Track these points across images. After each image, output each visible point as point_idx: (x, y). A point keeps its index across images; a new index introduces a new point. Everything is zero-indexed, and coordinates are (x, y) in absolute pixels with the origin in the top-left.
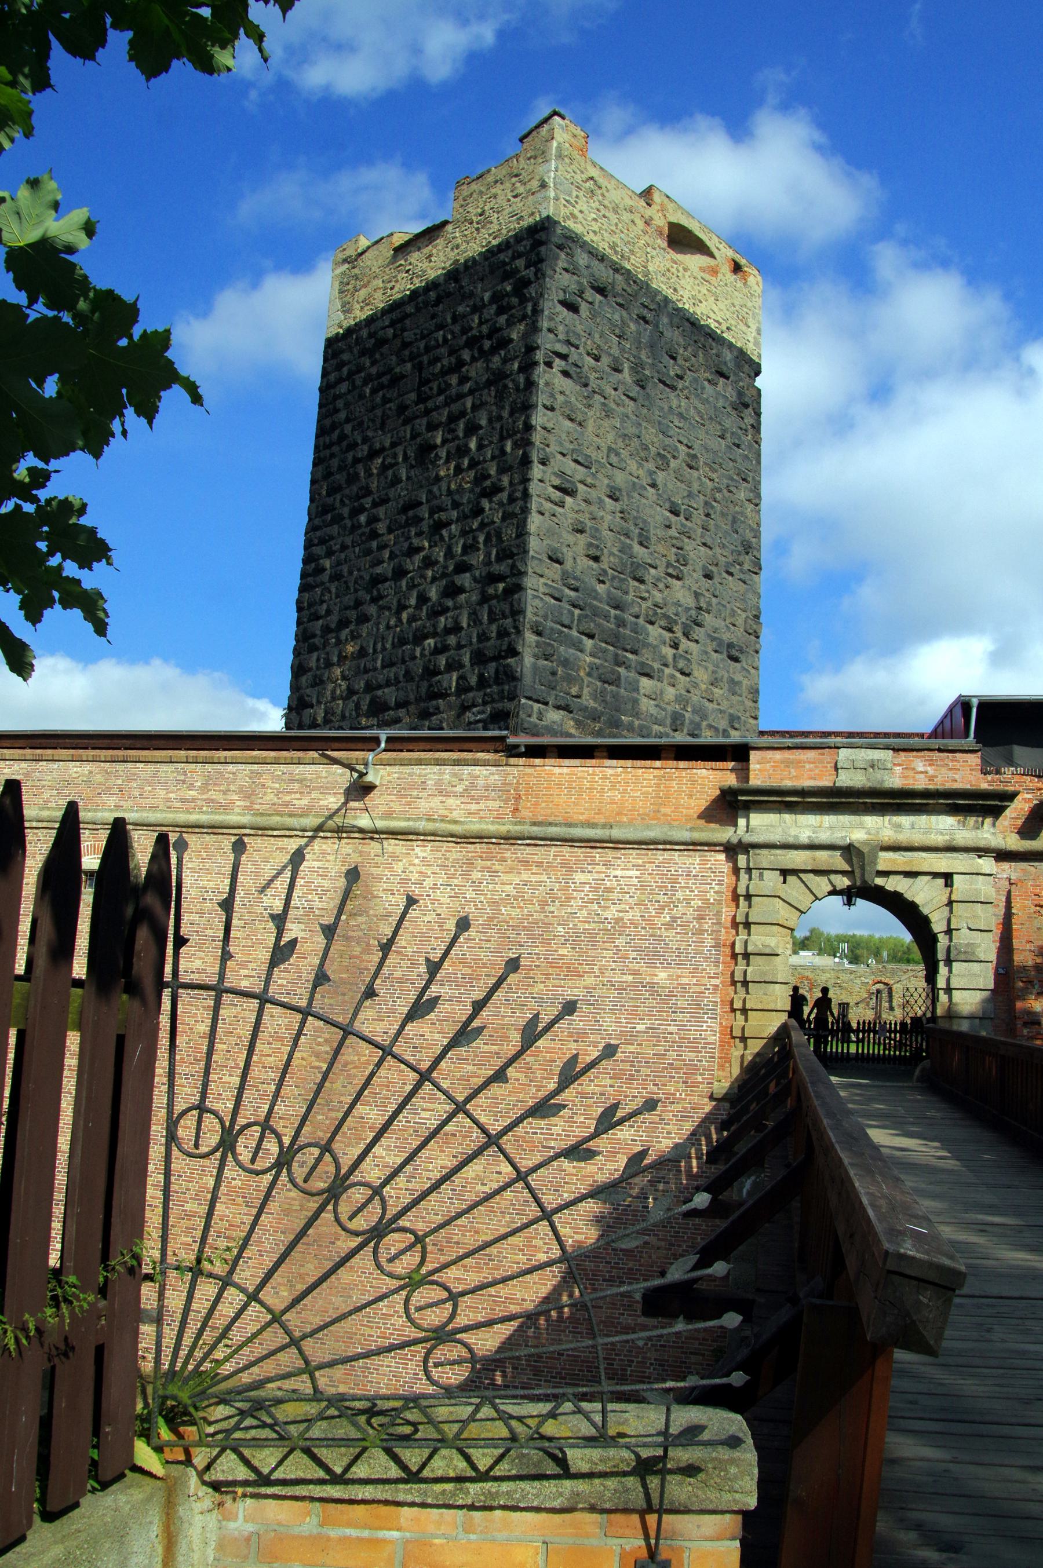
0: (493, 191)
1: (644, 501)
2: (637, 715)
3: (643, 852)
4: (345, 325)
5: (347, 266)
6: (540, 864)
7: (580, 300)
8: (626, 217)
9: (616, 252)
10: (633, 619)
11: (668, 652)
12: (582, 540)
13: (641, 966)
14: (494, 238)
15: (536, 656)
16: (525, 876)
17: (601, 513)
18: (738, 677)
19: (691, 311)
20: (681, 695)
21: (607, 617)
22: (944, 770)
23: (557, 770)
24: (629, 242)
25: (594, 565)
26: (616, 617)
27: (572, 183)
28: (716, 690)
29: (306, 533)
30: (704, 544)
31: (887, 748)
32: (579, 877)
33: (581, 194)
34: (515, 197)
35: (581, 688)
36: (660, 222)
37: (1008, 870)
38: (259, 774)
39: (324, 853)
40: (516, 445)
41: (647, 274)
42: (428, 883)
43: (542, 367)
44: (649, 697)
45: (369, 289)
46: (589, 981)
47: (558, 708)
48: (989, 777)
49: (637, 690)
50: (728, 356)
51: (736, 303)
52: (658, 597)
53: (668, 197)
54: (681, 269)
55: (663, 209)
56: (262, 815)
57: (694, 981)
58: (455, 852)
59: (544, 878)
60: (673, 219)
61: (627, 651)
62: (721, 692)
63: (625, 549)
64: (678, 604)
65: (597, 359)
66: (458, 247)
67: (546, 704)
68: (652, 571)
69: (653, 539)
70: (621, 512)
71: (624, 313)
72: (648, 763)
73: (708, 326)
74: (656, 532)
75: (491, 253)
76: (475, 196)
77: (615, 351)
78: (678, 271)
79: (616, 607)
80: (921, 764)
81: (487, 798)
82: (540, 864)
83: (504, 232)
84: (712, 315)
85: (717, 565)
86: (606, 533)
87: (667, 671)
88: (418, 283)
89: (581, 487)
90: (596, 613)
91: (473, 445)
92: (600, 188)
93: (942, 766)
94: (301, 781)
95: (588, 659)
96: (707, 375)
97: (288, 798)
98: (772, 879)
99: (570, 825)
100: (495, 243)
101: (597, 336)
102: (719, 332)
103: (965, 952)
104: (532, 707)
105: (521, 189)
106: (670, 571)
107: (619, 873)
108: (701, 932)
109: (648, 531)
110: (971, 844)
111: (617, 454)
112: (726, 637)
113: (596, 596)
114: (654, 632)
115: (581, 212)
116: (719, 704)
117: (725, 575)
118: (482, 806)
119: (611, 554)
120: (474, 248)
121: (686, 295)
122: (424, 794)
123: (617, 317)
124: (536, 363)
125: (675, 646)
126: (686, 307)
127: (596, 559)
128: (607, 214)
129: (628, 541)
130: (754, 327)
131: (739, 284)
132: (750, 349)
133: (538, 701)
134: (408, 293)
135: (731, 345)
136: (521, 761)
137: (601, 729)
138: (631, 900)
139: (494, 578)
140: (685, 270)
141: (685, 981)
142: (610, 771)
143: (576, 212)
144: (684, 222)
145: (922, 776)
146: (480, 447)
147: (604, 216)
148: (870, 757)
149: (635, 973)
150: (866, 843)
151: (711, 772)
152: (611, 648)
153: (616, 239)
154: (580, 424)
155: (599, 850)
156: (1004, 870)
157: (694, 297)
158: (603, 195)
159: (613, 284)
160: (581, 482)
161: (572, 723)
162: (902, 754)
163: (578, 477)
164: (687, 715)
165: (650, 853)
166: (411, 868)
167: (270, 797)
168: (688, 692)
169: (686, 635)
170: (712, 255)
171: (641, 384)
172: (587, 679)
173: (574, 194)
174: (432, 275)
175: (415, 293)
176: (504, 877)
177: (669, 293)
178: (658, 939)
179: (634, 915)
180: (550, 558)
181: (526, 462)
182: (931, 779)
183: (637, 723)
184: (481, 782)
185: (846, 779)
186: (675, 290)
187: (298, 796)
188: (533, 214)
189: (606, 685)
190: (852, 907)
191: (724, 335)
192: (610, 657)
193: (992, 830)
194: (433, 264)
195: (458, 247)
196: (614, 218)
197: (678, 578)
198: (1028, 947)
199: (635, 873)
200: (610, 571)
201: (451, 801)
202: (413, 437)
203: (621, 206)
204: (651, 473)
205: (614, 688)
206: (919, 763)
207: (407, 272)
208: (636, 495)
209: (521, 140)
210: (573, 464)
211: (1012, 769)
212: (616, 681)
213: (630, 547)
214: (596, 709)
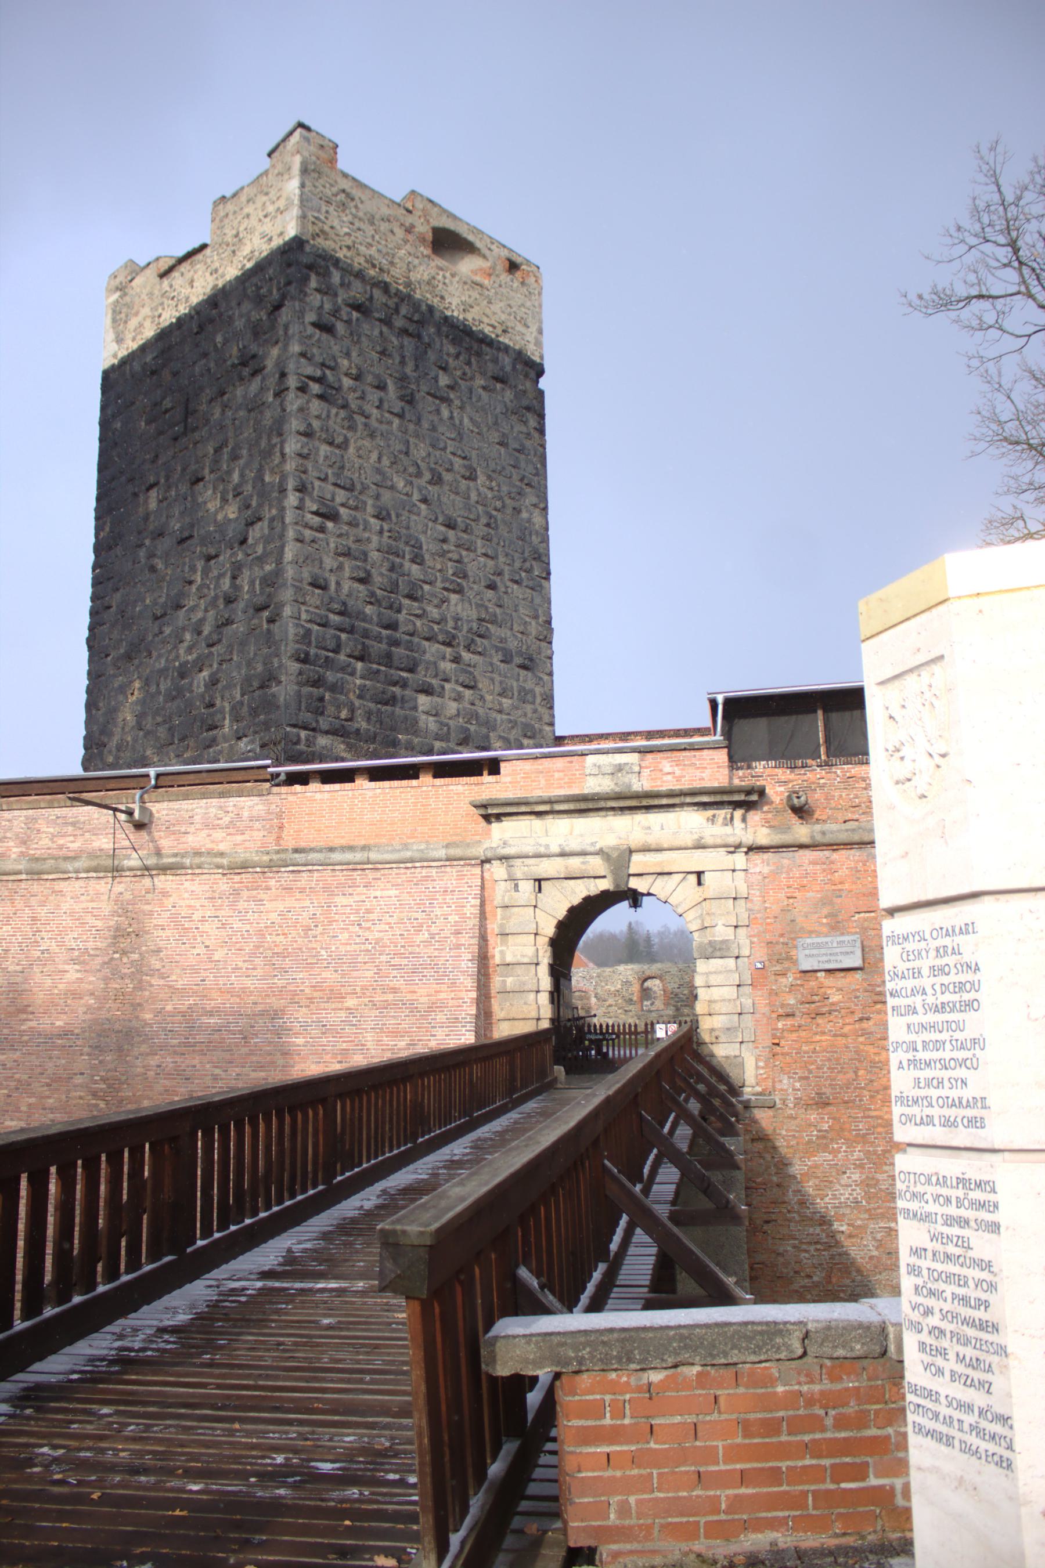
0: (246, 211)
1: (414, 517)
3: (403, 871)
4: (120, 355)
5: (118, 294)
6: (302, 890)
7: (333, 319)
8: (384, 227)
9: (374, 266)
10: (408, 638)
11: (447, 666)
12: (348, 564)
13: (399, 983)
14: (249, 260)
15: (298, 683)
17: (366, 535)
18: (529, 685)
19: (461, 317)
20: (464, 709)
21: (379, 639)
22: (691, 770)
23: (318, 796)
24: (387, 254)
25: (361, 587)
26: (388, 637)
27: (321, 199)
28: (504, 700)
29: (94, 569)
30: (485, 555)
31: (634, 750)
32: (341, 900)
33: (331, 209)
34: (266, 216)
35: (352, 710)
36: (423, 229)
37: (761, 864)
38: (35, 820)
39: (98, 894)
41: (408, 284)
43: (291, 395)
44: (427, 713)
45: (140, 318)
47: (327, 732)
48: (741, 773)
49: (415, 708)
50: (506, 361)
51: (512, 303)
53: (431, 201)
54: (448, 275)
55: (425, 214)
56: (37, 860)
57: (453, 995)
59: (307, 903)
61: (401, 670)
62: (510, 701)
64: (457, 619)
65: (357, 378)
66: (216, 271)
67: (314, 730)
68: (426, 587)
69: (427, 557)
70: (389, 531)
71: (385, 329)
72: (405, 783)
73: (482, 332)
74: (429, 546)
75: (246, 277)
76: (231, 217)
77: (377, 370)
78: (444, 277)
79: (387, 627)
80: (668, 765)
81: (251, 828)
82: (302, 890)
83: (257, 254)
84: (486, 320)
85: (499, 574)
86: (374, 555)
87: (447, 686)
88: (183, 309)
89: (342, 511)
90: (366, 634)
91: (236, 477)
92: (353, 199)
93: (690, 765)
94: (73, 824)
95: (358, 682)
96: (482, 382)
97: (61, 842)
98: (527, 887)
99: (331, 850)
100: (249, 265)
101: (354, 354)
102: (493, 336)
103: (720, 949)
104: (298, 736)
105: (271, 208)
106: (447, 585)
107: (378, 894)
108: (458, 946)
109: (421, 548)
110: (719, 841)
114: (432, 649)
115: (332, 227)
116: (509, 714)
117: (509, 584)
118: (246, 837)
119: (382, 575)
120: (232, 272)
122: (192, 829)
123: (376, 332)
124: (287, 389)
125: (456, 660)
126: (455, 314)
127: (362, 581)
128: (362, 226)
129: (398, 560)
130: (534, 329)
132: (532, 352)
133: (305, 728)
134: (174, 320)
135: (506, 349)
136: (284, 789)
137: (375, 749)
138: (390, 920)
139: (260, 609)
140: (453, 275)
141: (443, 996)
142: (370, 793)
143: (326, 228)
144: (450, 225)
145: (669, 777)
146: (242, 475)
147: (359, 229)
148: (617, 762)
149: (395, 990)
150: (614, 848)
151: (466, 787)
152: (383, 668)
153: (373, 251)
154: (338, 447)
155: (359, 872)
156: (756, 865)
157: (463, 303)
158: (356, 207)
159: (371, 299)
160: (343, 505)
161: (342, 746)
162: (649, 756)
163: (339, 500)
164: (472, 728)
165: (408, 871)
166: (182, 903)
167: (45, 842)
168: (473, 704)
169: (468, 648)
171: (409, 400)
172: (357, 703)
173: (324, 209)
174: (195, 300)
175: (180, 322)
176: (269, 906)
177: (436, 301)
180: (311, 584)
181: (283, 491)
182: (678, 779)
183: (416, 740)
184: (246, 814)
185: (594, 785)
186: (442, 298)
187: (72, 838)
188: (281, 234)
189: (379, 706)
190: (638, 909)
191: (501, 339)
192: (382, 677)
193: (743, 825)
194: (196, 287)
195: (216, 271)
196: (370, 230)
197: (454, 592)
198: (781, 940)
199: (393, 892)
200: (379, 592)
201: (219, 835)
203: (377, 217)
205: (388, 708)
206: (666, 764)
207: (173, 298)
208: (406, 513)
209: (269, 155)
210: (331, 488)
211: (762, 763)
212: (392, 701)
213: (401, 565)
214: (369, 730)
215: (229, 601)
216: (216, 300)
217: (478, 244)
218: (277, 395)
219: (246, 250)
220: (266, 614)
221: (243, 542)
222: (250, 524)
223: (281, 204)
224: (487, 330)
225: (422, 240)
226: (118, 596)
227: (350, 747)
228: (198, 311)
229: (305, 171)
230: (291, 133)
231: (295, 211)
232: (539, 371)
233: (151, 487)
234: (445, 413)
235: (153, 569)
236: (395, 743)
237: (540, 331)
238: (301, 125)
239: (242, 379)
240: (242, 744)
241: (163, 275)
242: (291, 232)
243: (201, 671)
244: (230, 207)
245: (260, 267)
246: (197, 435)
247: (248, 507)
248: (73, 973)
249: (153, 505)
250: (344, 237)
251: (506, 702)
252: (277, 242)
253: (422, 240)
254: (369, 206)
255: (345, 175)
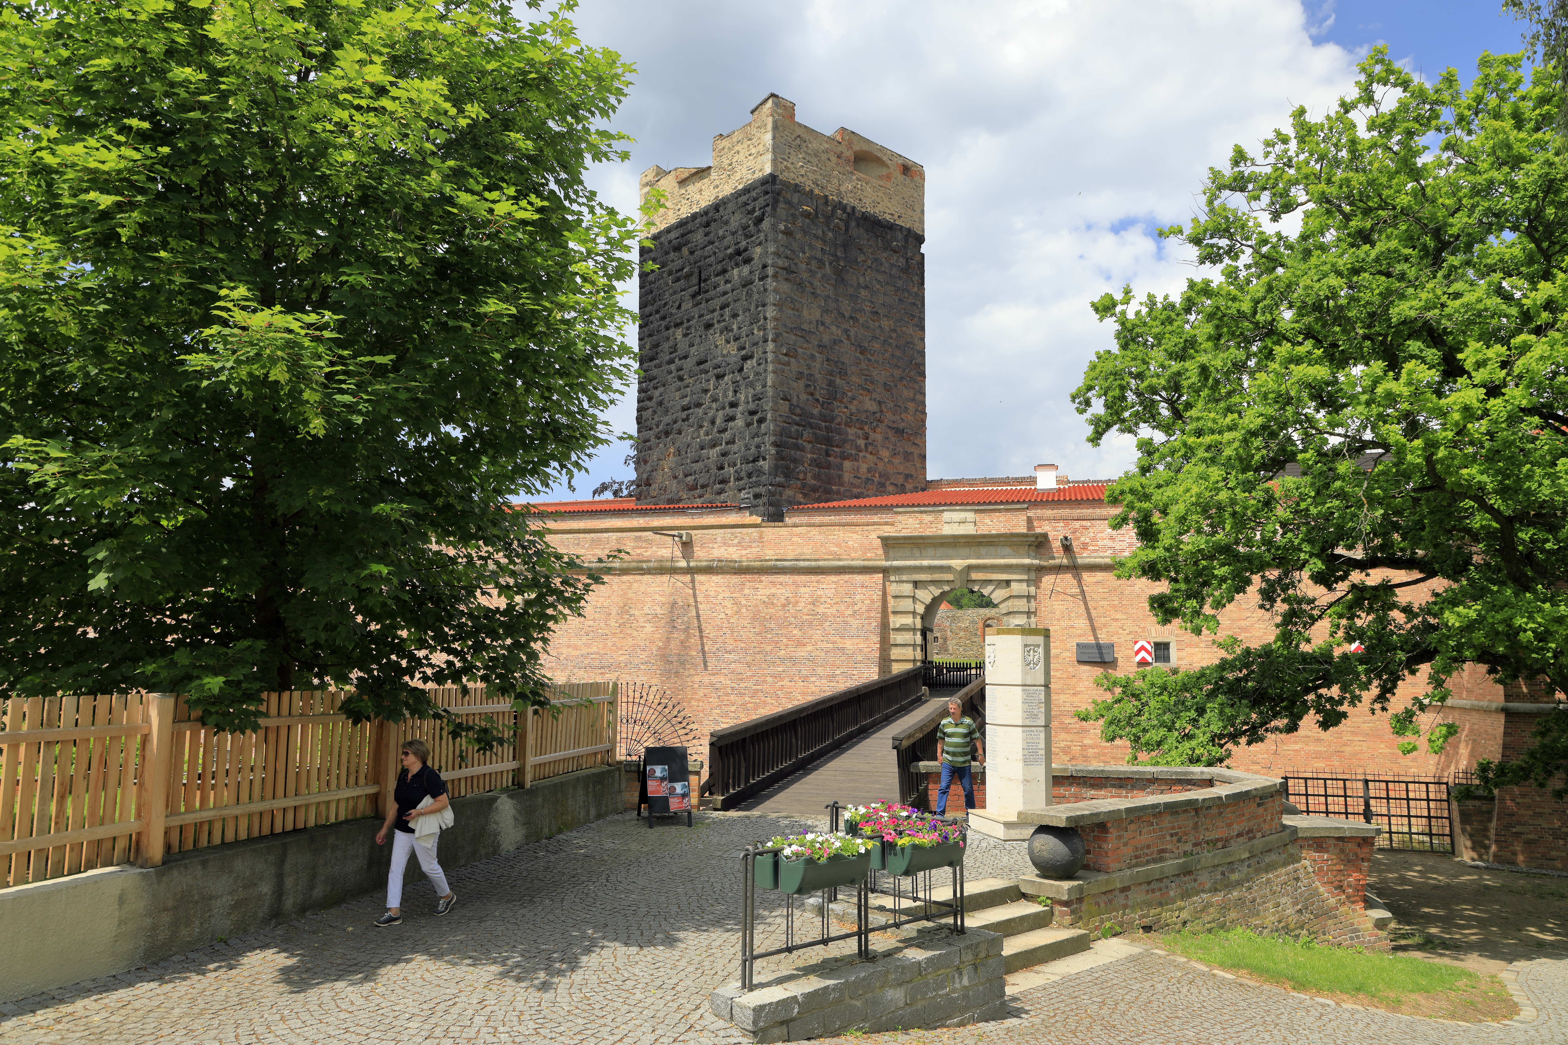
2: (842, 485)
11: (861, 442)
12: (802, 383)
16: (773, 590)
32: (802, 590)
36: (848, 154)
40: (759, 329)
41: (839, 194)
42: (720, 597)
46: (809, 648)
52: (853, 408)
55: (850, 142)
58: (735, 579)
60: (857, 148)
63: (831, 383)
75: (738, 194)
86: (818, 376)
88: (696, 209)
89: (800, 351)
91: (735, 327)
100: (740, 187)
105: (753, 151)
111: (823, 324)
112: (901, 426)
113: (812, 416)
114: (851, 431)
120: (727, 190)
121: (867, 201)
123: (820, 232)
130: (918, 211)
131: (908, 181)
132: (916, 229)
144: (866, 148)
149: (834, 642)
170: (887, 166)
171: (839, 273)
174: (704, 204)
175: (694, 216)
177: (856, 203)
178: (846, 623)
179: (833, 610)
196: (814, 160)
201: (731, 550)
202: (701, 316)
204: (846, 331)
209: (752, 112)
215: (733, 405)
216: (717, 206)
217: (885, 158)
218: (761, 279)
219: (738, 176)
220: (756, 418)
221: (741, 370)
222: (745, 358)
223: (761, 148)
224: (888, 217)
225: (848, 161)
226: (657, 393)
227: (805, 495)
228: (705, 212)
229: (775, 128)
230: (766, 100)
231: (769, 156)
232: (920, 239)
233: (677, 325)
234: (862, 280)
235: (681, 379)
236: (828, 492)
237: (923, 212)
238: (773, 95)
239: (737, 265)
240: (743, 495)
241: (683, 182)
242: (768, 170)
243: (714, 446)
244: (725, 143)
245: (747, 190)
246: (707, 295)
247: (744, 348)
248: (649, 628)
249: (679, 337)
250: (800, 171)
251: (896, 461)
252: (758, 175)
253: (848, 161)
254: (814, 145)
255: (800, 125)
